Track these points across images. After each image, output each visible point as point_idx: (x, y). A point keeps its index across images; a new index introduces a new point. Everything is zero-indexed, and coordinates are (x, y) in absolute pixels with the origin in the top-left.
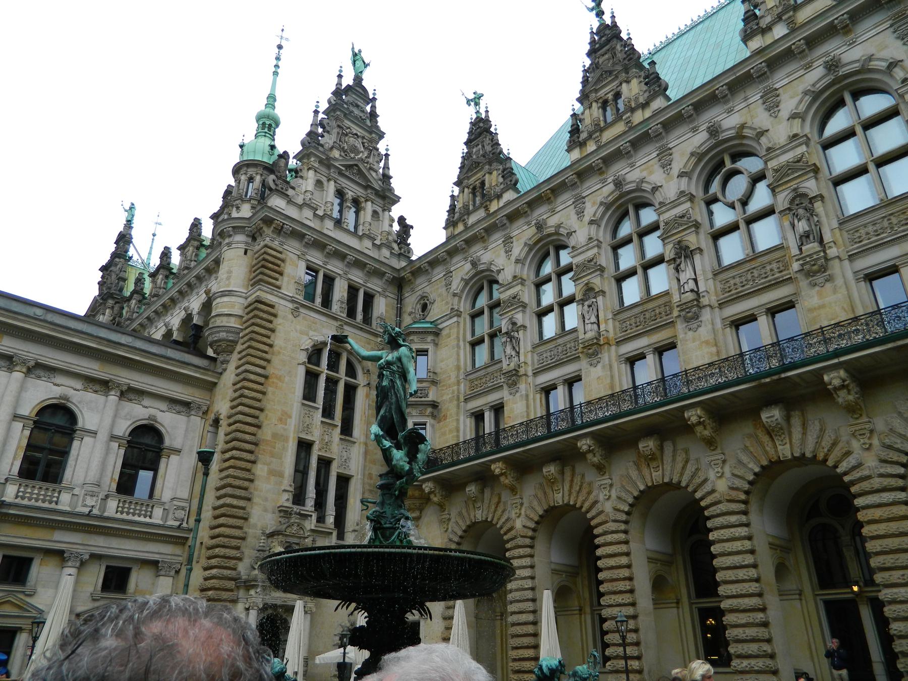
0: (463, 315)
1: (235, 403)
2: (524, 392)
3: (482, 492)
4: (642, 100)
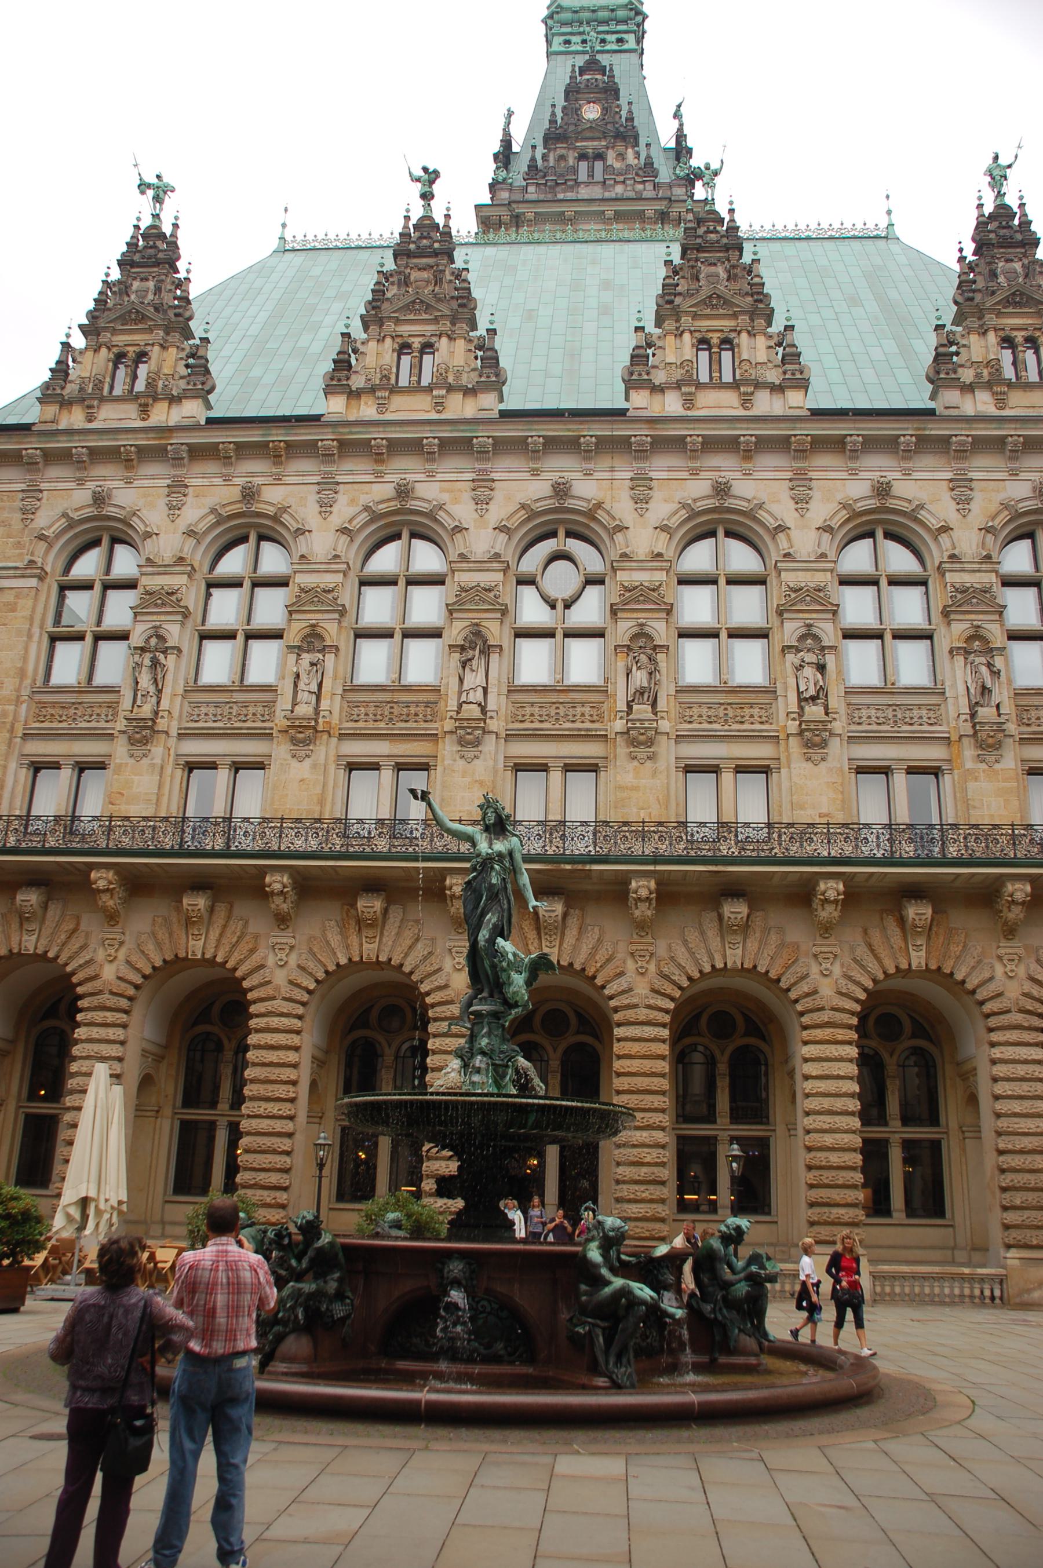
0: (48, 580)
2: (158, 761)
4: (469, 379)
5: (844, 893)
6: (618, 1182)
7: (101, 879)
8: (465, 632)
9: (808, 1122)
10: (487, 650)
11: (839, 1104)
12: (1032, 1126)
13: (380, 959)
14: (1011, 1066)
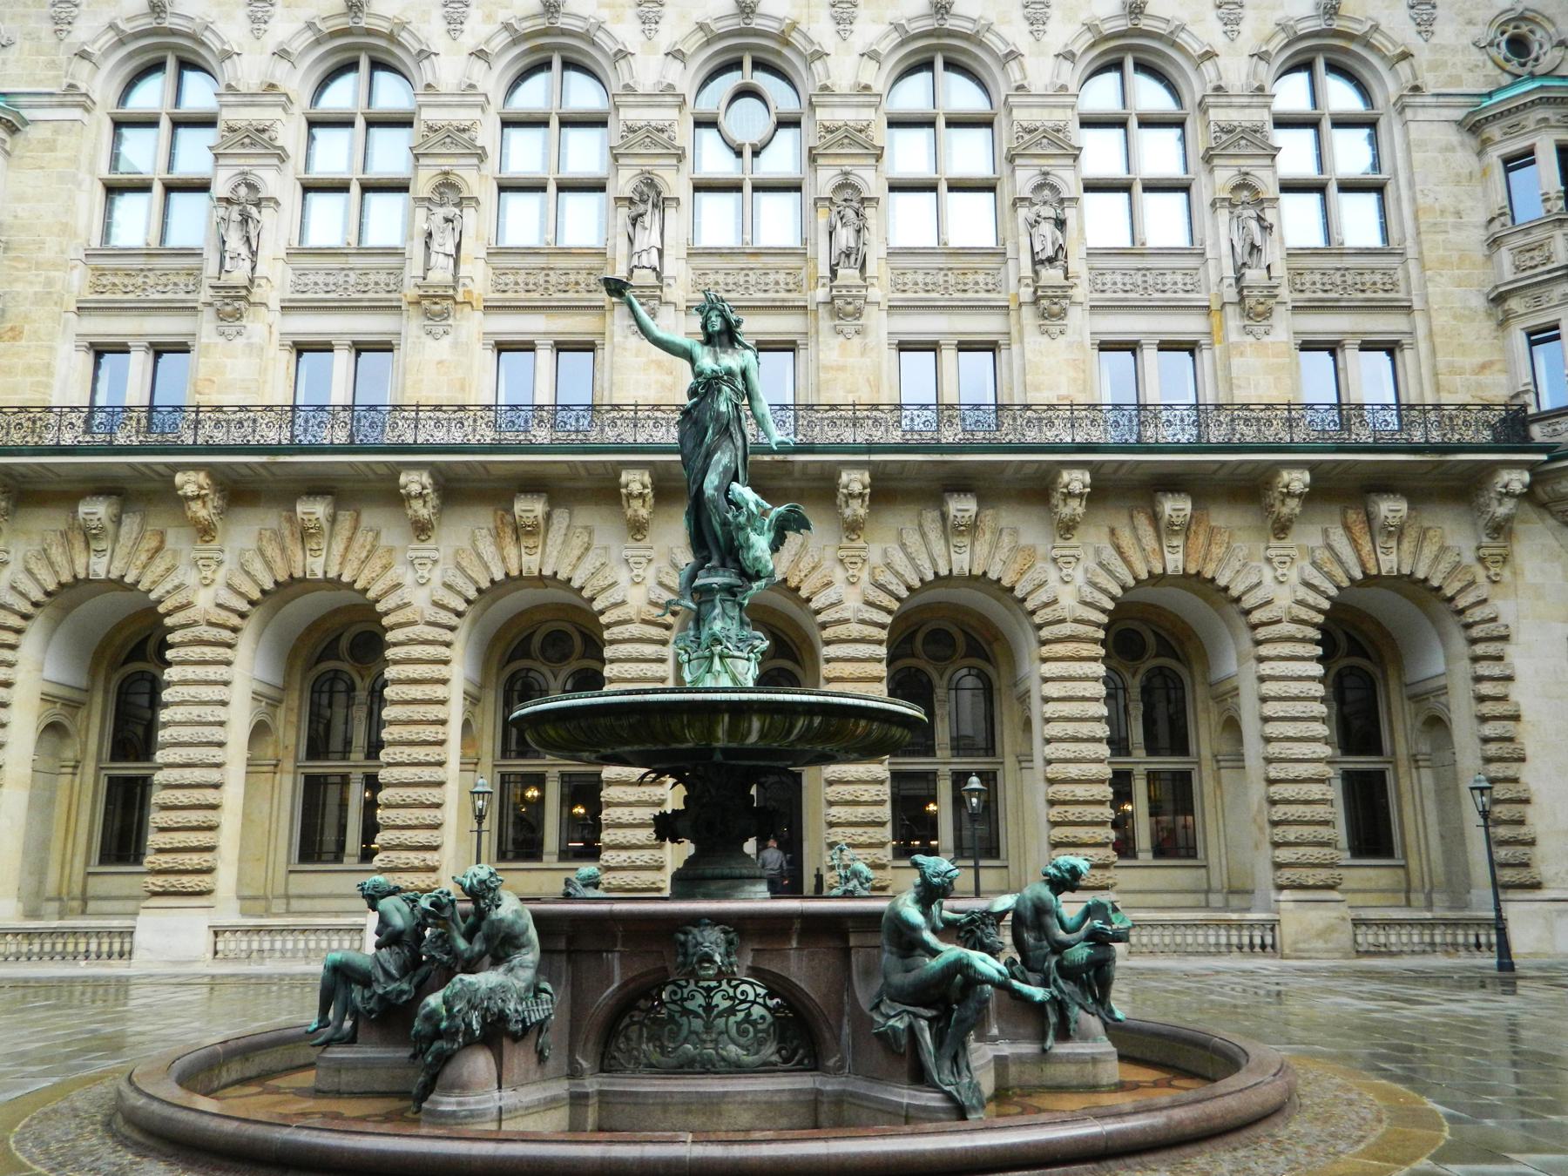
3: (118, 521)
5: (1091, 486)
6: (831, 825)
7: (189, 483)
8: (635, 182)
9: (1051, 750)
10: (661, 203)
11: (1085, 729)
12: (1307, 752)
13: (544, 573)
14: (1282, 683)
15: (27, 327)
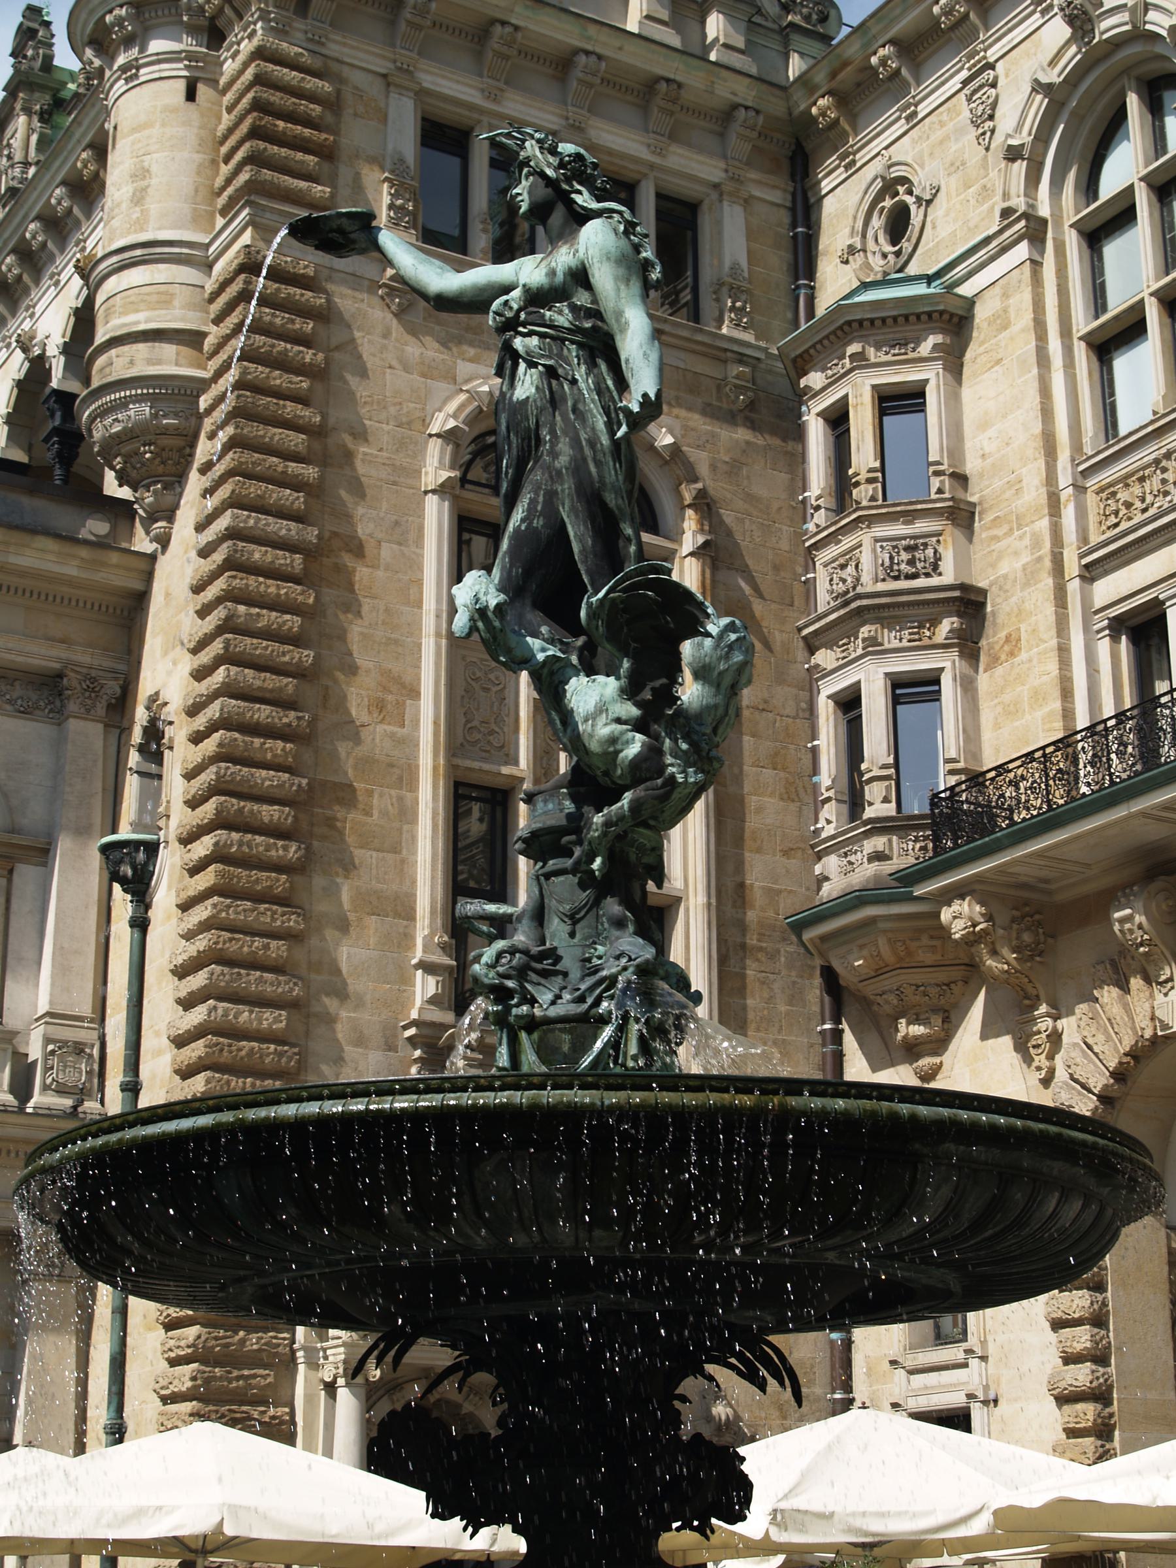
1: (206, 657)
15: (1023, 627)
